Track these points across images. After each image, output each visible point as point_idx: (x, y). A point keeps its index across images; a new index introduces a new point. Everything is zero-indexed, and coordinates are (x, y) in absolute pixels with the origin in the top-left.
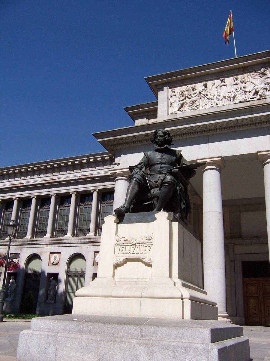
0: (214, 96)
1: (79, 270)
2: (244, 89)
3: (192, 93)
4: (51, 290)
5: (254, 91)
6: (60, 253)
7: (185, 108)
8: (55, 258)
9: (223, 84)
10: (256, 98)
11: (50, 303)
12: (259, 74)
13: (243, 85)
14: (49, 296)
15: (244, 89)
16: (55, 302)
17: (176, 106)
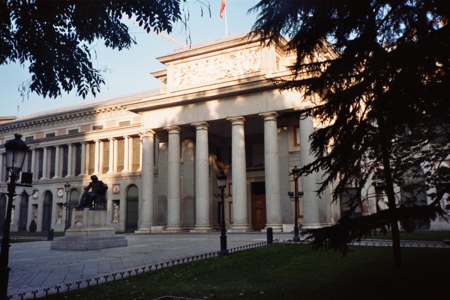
0: (202, 73)
1: (134, 196)
2: (221, 68)
3: (189, 70)
4: (115, 213)
5: (227, 71)
6: (120, 184)
7: (184, 83)
8: (116, 189)
9: (208, 63)
10: (227, 76)
11: (115, 223)
12: (230, 55)
13: (221, 65)
14: (114, 217)
15: (222, 69)
16: (119, 221)
17: (179, 80)
